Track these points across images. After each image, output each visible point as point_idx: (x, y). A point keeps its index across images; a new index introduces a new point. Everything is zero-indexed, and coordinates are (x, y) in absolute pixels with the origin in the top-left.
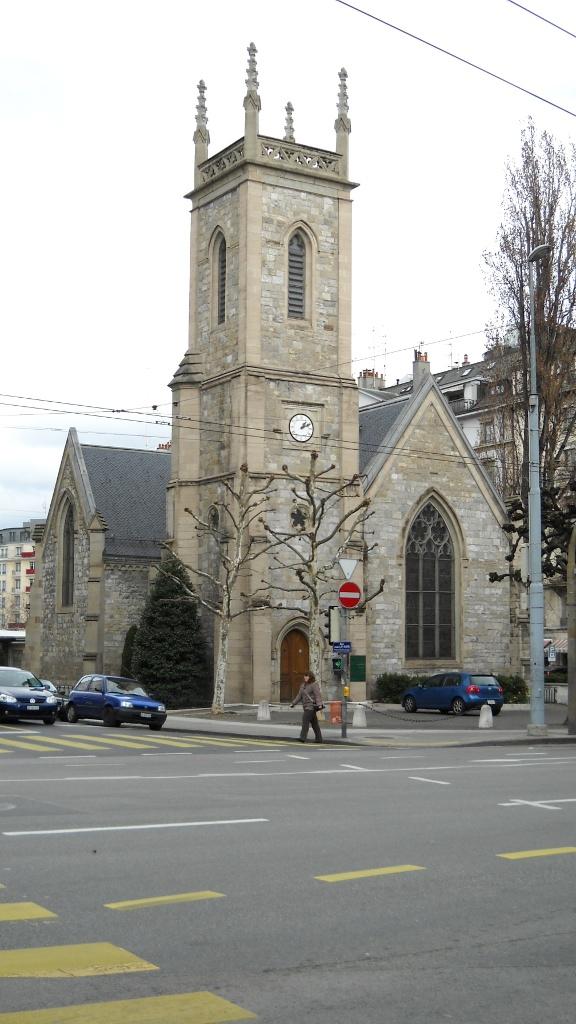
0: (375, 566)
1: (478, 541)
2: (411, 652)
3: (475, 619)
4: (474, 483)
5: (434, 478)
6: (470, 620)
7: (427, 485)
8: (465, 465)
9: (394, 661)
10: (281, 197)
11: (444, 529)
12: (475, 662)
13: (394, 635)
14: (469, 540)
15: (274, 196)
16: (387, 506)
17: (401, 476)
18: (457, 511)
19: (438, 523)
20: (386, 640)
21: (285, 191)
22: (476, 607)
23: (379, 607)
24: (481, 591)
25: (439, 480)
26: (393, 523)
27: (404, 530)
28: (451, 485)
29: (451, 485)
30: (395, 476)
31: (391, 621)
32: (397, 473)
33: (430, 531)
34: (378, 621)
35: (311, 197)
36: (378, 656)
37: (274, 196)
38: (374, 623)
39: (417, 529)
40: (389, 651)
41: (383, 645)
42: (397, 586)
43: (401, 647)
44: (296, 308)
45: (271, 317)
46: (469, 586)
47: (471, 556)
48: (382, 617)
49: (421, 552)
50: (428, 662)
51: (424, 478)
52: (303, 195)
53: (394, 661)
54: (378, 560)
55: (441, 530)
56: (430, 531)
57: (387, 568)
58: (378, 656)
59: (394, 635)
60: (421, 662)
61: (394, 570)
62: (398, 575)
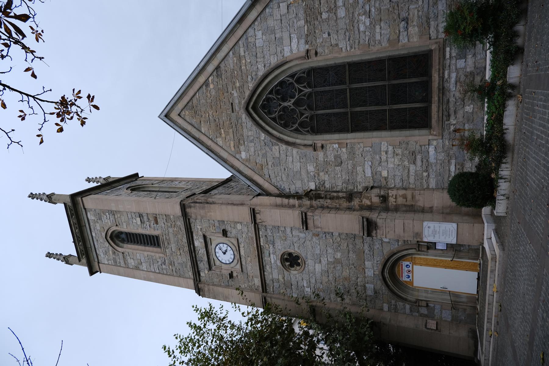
0: (326, 178)
1: (286, 41)
2: (419, 120)
3: (378, 27)
4: (231, 53)
5: (236, 107)
6: (378, 37)
7: (244, 116)
8: (218, 68)
9: (432, 150)
10: (101, 250)
11: (282, 83)
12: (436, 17)
13: (399, 151)
14: (287, 53)
15: (102, 255)
16: (270, 163)
17: (242, 148)
18: (261, 73)
19: (277, 93)
20: (406, 163)
21: (96, 247)
22: (362, 28)
23: (369, 173)
24: (342, 24)
25: (237, 101)
26: (283, 156)
27: (288, 143)
28: (238, 85)
29: (238, 85)
30: (243, 155)
31: (384, 157)
32: (240, 153)
33: (286, 104)
34: (385, 174)
35: (92, 230)
36: (425, 174)
37: (102, 255)
38: (386, 179)
39: (286, 120)
40: (419, 157)
41: (412, 168)
42: (344, 150)
43: (417, 137)
44: (152, 241)
45: (164, 266)
46: (337, 45)
47: (303, 48)
48: (379, 169)
49: (307, 114)
50: (435, 98)
51: (238, 118)
52: (94, 235)
53: (432, 150)
54: (321, 174)
55: (283, 89)
56: (286, 104)
57: (327, 163)
58: (425, 174)
59: (399, 151)
60: (434, 108)
61: (328, 153)
62: (334, 149)
